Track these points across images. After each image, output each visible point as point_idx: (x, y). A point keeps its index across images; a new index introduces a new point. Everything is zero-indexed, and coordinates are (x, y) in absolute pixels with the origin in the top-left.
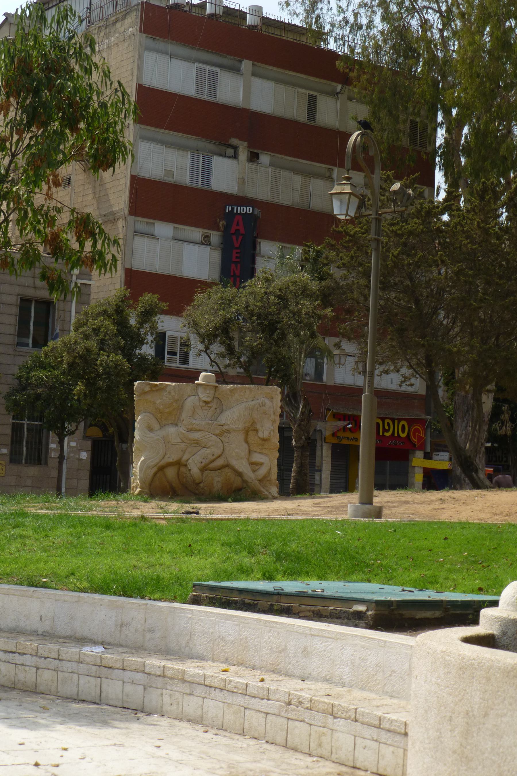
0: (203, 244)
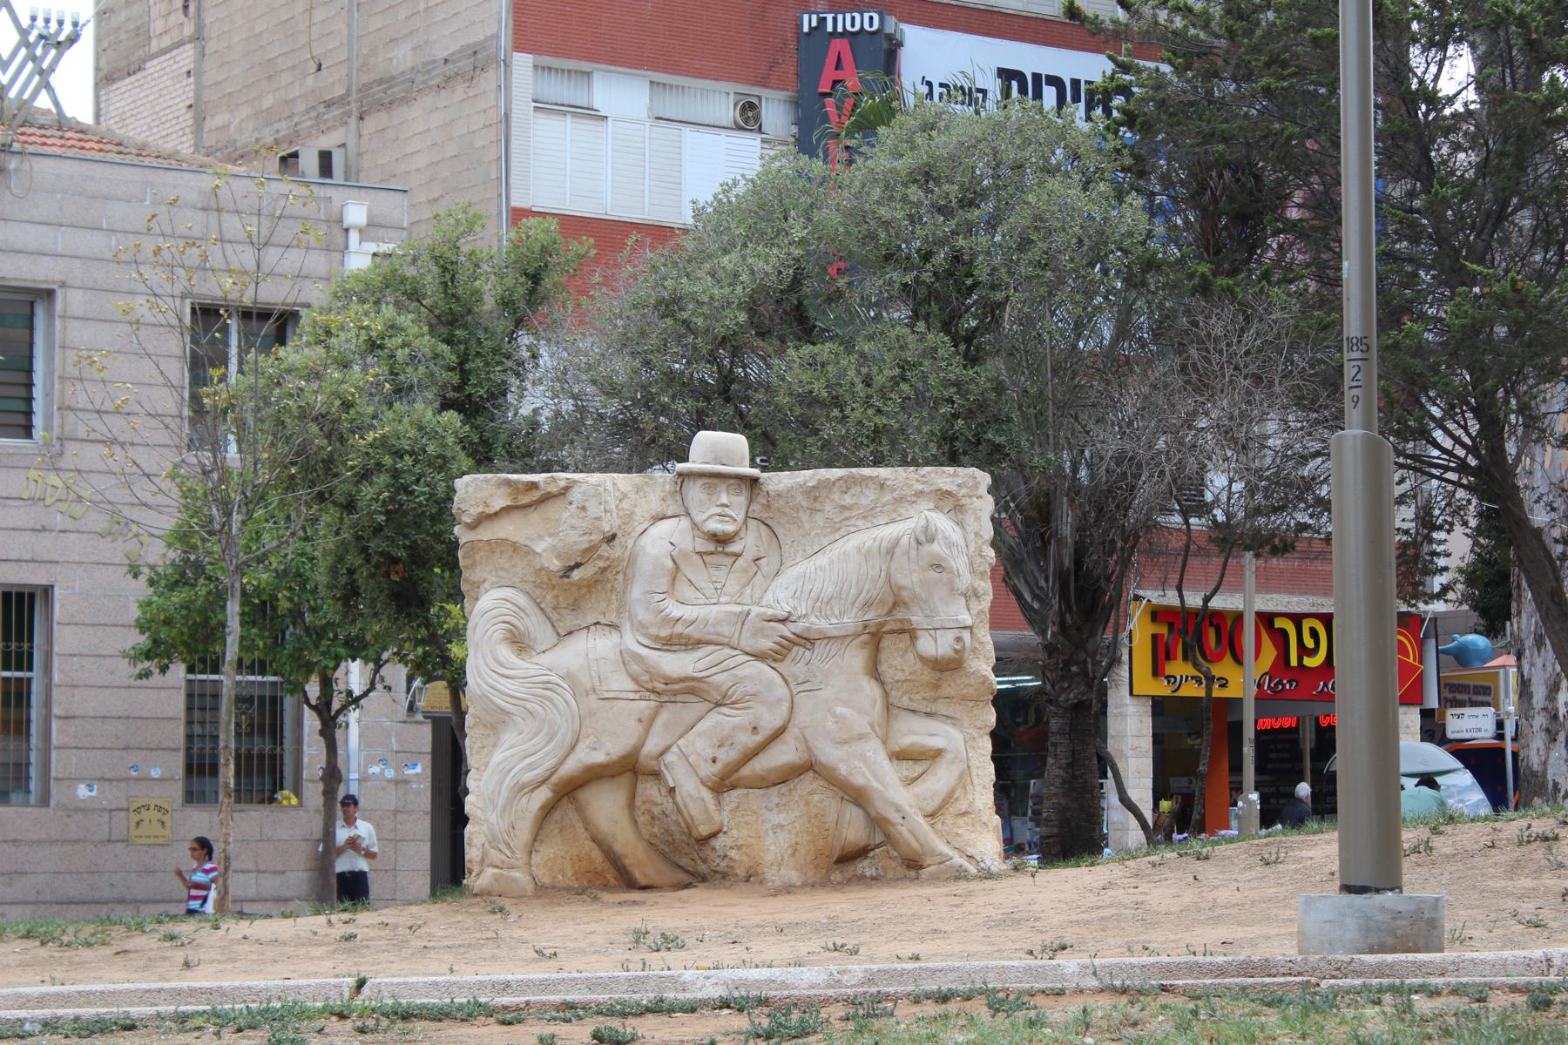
0: (740, 128)
